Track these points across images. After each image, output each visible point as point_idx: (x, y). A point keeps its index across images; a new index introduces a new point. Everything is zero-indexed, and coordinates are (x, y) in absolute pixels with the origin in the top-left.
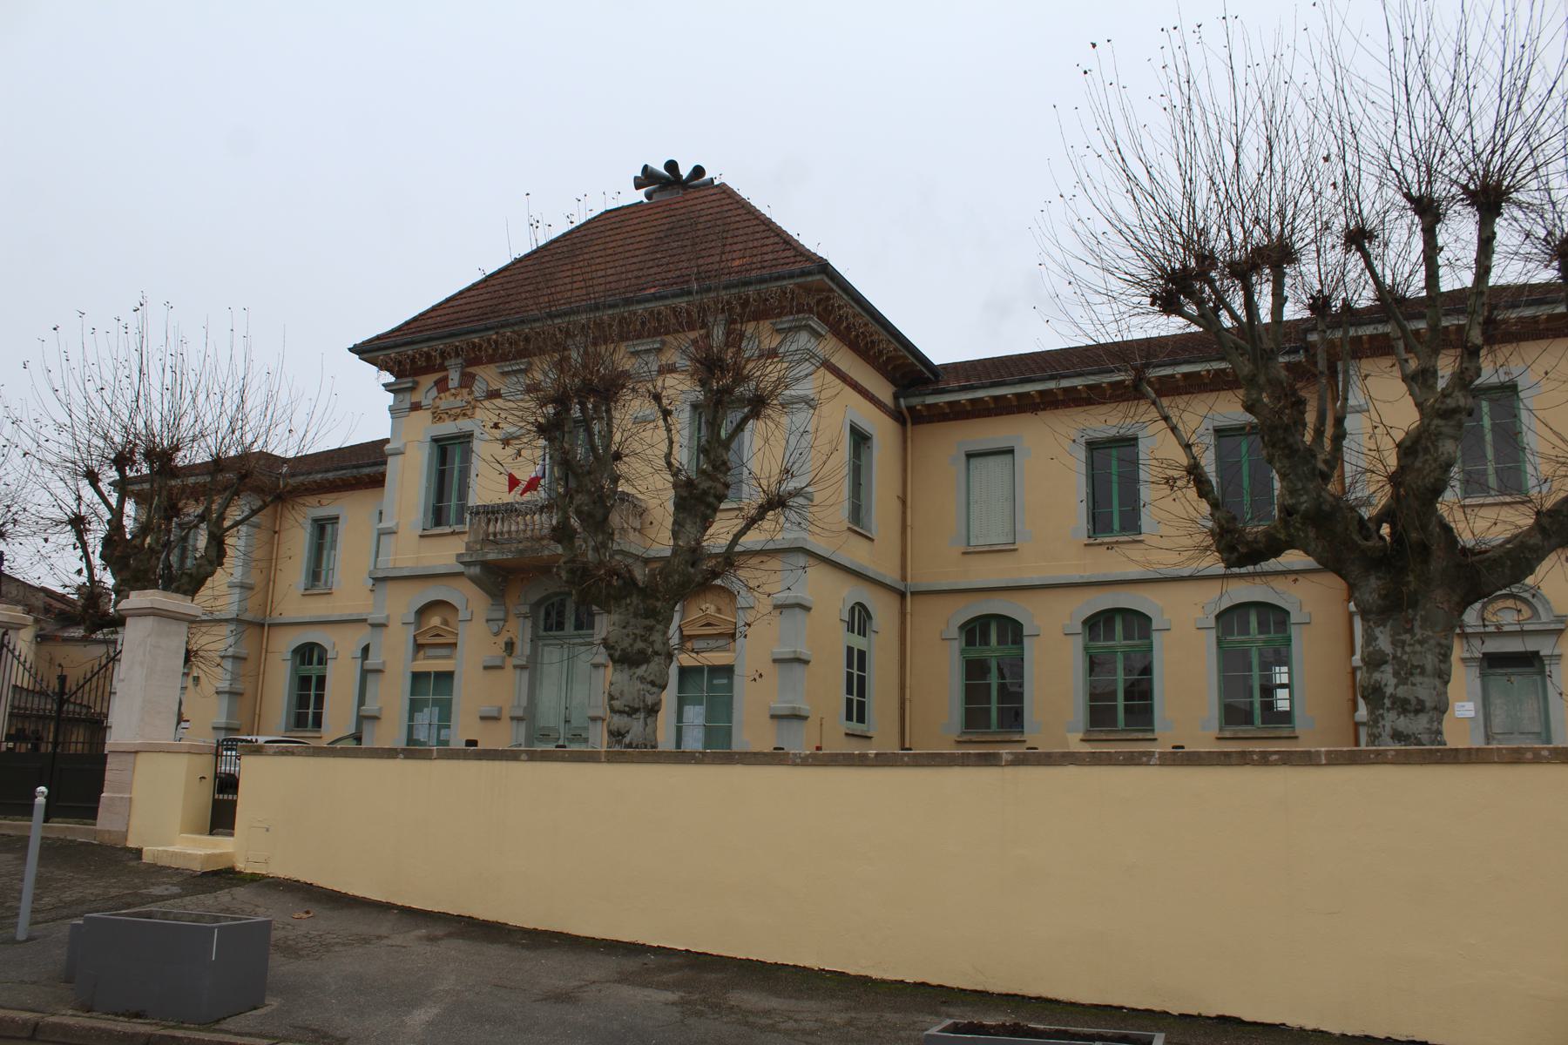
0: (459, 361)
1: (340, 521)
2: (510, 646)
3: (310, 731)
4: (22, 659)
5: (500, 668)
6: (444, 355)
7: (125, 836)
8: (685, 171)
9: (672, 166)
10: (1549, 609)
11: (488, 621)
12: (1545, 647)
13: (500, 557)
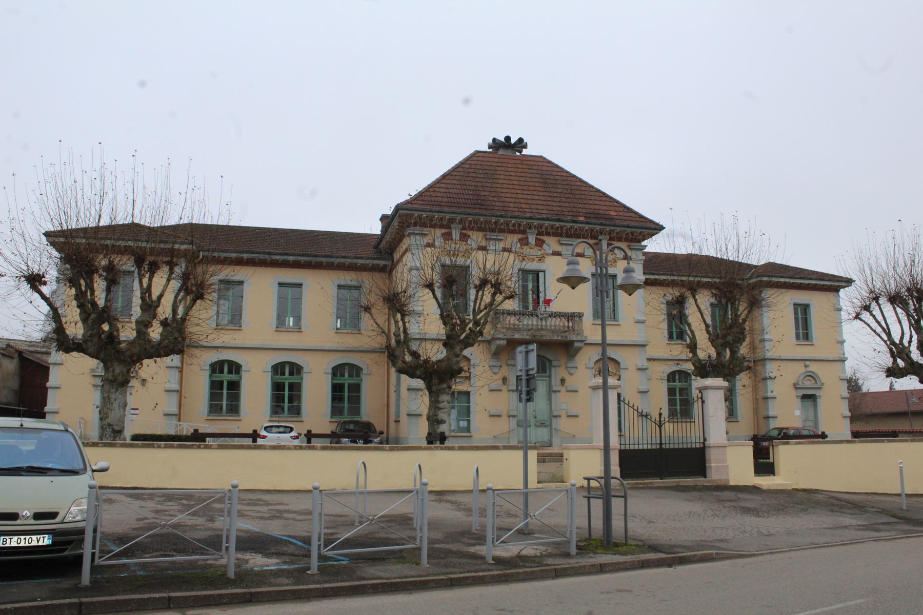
0: (461, 226)
1: (245, 284)
2: (505, 380)
3: (225, 416)
4: (631, 405)
5: (500, 390)
6: (452, 221)
7: (728, 480)
8: (513, 141)
9: (508, 139)
10: (820, 381)
11: (490, 367)
12: (817, 393)
13: (522, 337)
